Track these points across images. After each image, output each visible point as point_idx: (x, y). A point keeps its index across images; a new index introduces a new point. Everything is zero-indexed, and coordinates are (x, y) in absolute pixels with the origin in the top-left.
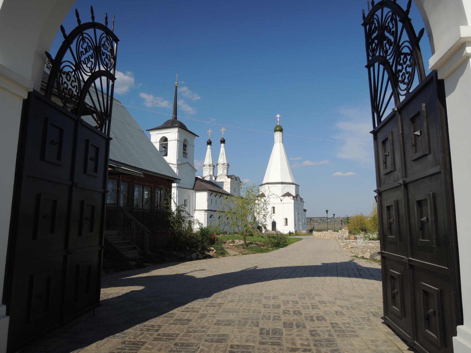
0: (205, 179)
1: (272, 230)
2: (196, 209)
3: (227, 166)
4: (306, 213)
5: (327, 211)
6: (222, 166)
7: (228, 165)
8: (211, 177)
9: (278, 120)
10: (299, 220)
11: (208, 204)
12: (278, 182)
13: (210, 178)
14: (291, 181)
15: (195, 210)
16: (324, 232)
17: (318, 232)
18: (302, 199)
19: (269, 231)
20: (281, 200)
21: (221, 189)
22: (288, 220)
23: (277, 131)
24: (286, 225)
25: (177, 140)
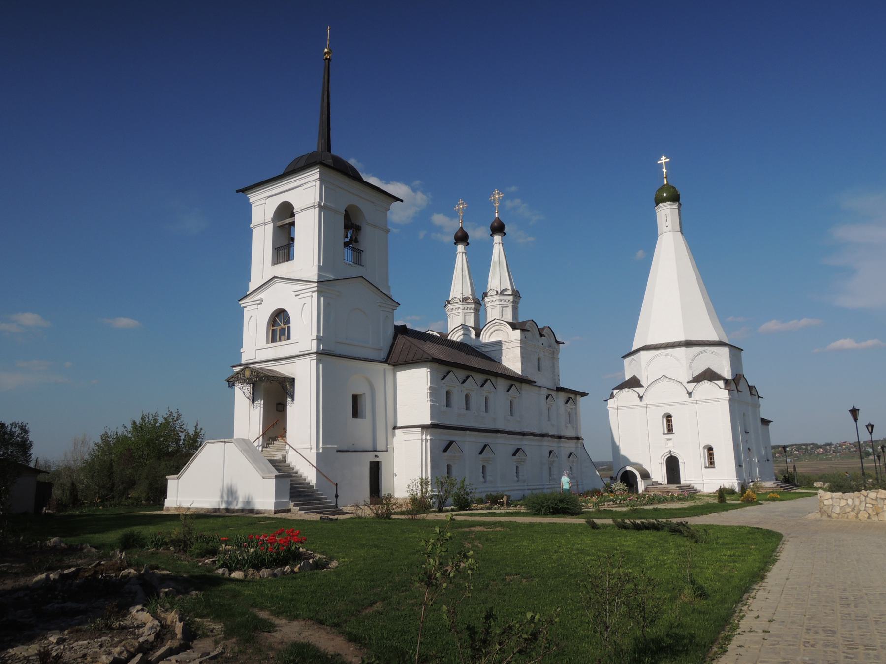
0: (449, 338)
1: (669, 483)
2: (399, 425)
3: (511, 298)
4: (768, 428)
5: (854, 412)
6: (497, 297)
7: (516, 294)
8: (467, 332)
9: (665, 170)
10: (749, 449)
11: (432, 406)
12: (675, 342)
13: (463, 334)
14: (715, 338)
15: (395, 428)
16: (872, 494)
17: (843, 493)
18: (754, 388)
19: (661, 484)
20: (690, 394)
21: (492, 363)
22: (714, 449)
23: (664, 200)
24: (709, 467)
25: (320, 205)
